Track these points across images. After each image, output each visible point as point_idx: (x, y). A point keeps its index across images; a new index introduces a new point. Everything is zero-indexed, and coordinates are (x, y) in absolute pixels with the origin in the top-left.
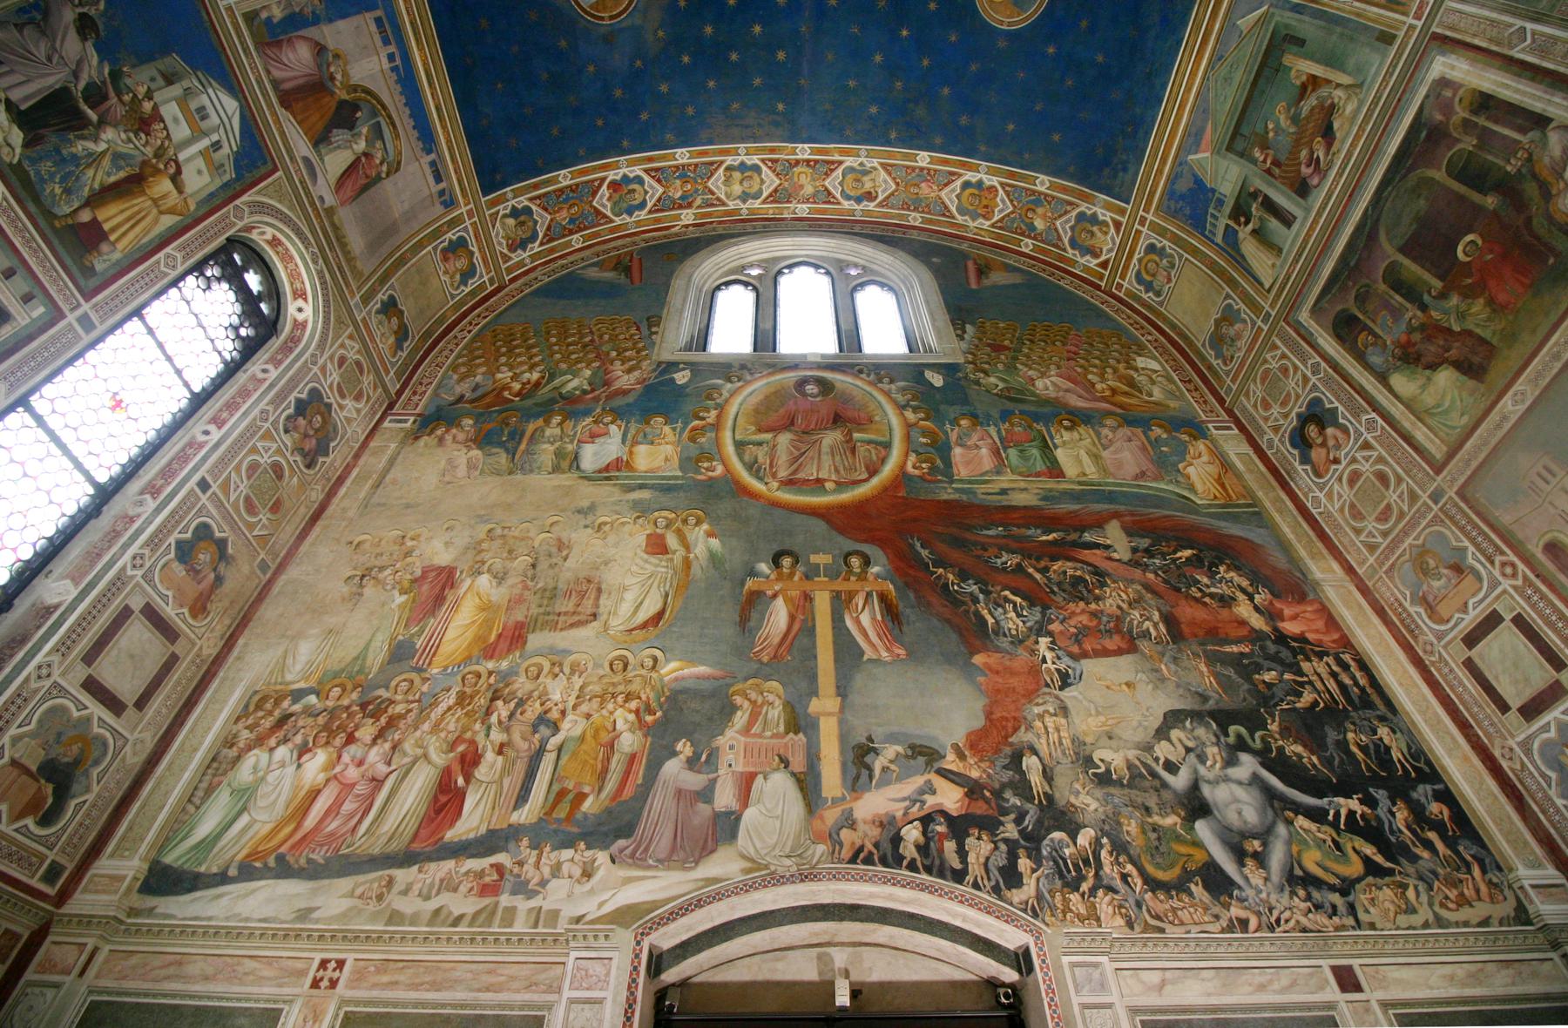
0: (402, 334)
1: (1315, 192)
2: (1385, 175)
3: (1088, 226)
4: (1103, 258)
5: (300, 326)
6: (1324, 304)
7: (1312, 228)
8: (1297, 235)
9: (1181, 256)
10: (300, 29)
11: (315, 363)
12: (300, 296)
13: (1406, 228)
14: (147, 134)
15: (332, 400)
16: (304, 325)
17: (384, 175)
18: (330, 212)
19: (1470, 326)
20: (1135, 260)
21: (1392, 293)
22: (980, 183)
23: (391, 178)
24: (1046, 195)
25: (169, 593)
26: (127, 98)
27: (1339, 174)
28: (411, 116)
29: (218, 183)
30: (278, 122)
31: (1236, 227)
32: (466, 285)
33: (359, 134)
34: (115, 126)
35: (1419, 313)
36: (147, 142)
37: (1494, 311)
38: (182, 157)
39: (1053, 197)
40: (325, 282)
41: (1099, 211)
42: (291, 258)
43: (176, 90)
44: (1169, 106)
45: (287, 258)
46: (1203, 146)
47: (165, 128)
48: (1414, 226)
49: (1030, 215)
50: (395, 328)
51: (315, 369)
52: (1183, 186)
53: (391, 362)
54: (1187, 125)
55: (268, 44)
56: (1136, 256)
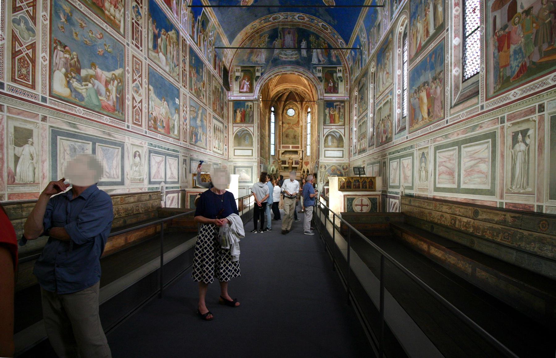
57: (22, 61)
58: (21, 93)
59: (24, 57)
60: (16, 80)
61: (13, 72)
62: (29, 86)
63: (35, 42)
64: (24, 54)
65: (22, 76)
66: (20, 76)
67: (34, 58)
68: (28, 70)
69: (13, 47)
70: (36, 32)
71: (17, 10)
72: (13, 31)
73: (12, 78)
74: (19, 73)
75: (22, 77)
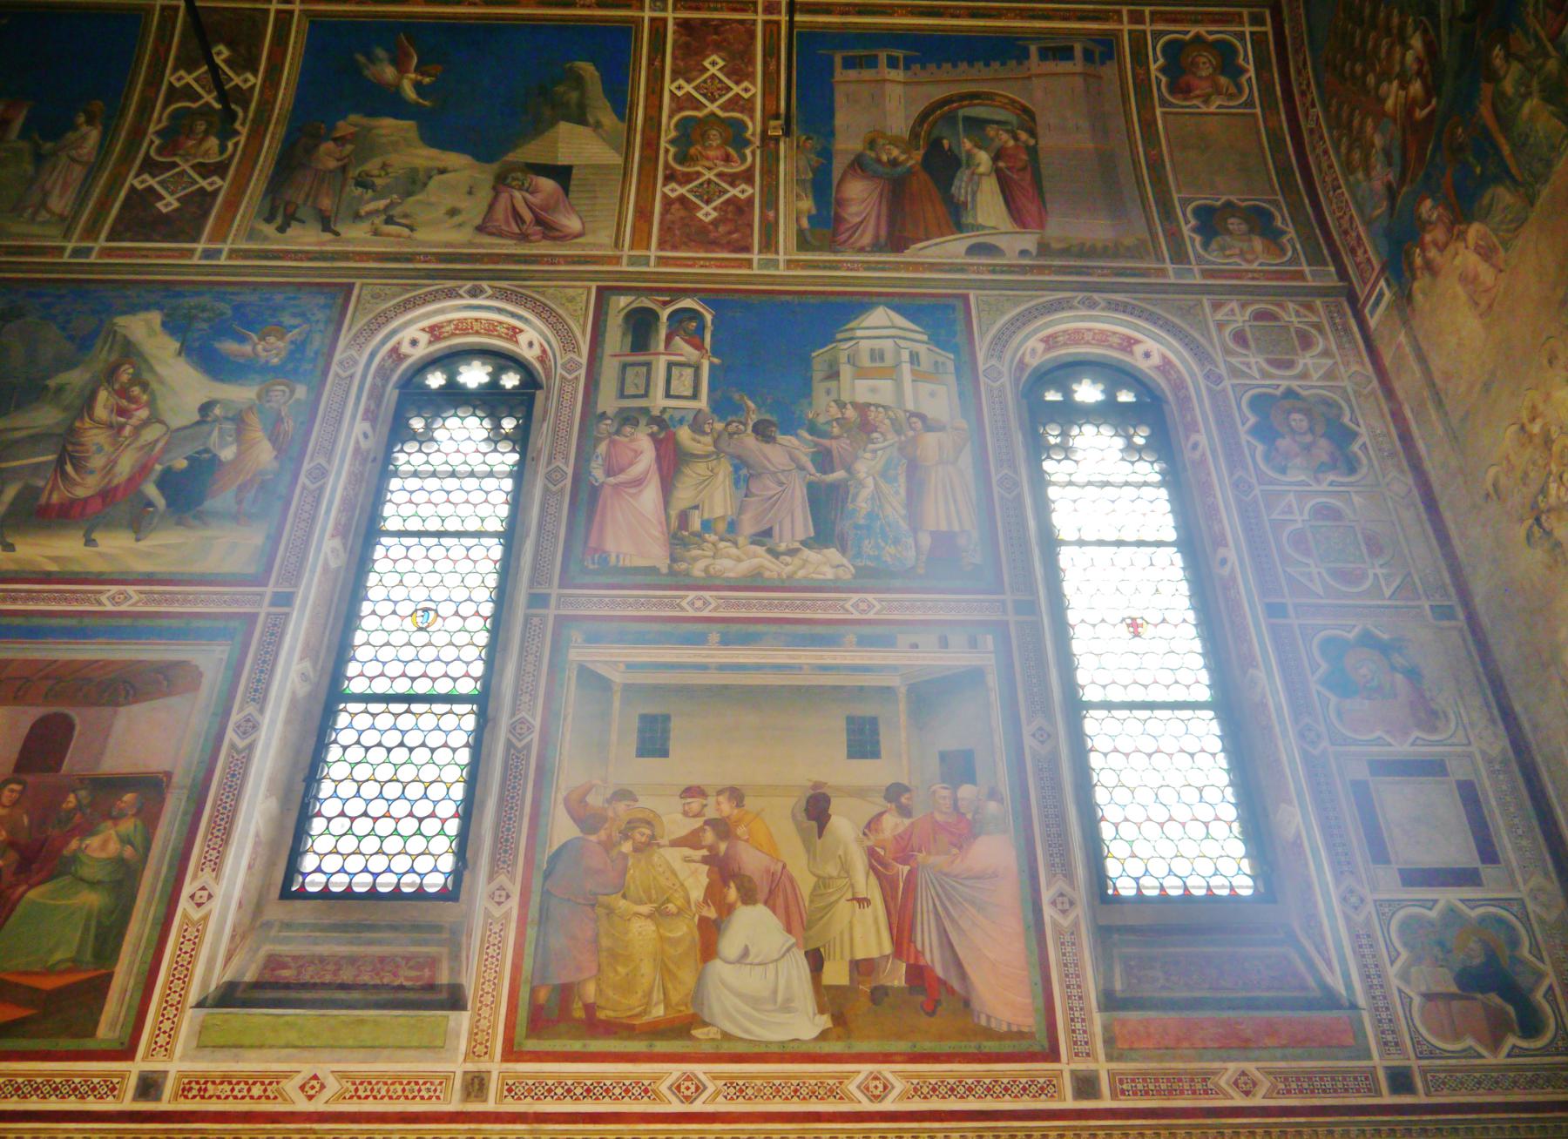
0: (1260, 221)
5: (1166, 366)
10: (830, 183)
11: (1220, 379)
12: (1131, 345)
14: (875, 429)
15: (1285, 384)
16: (1166, 361)
17: (1032, 142)
18: (1044, 249)
23: (1040, 131)
25: (1378, 734)
26: (836, 431)
28: (971, 63)
29: (951, 379)
30: (917, 266)
32: (1243, 71)
33: (970, 155)
34: (856, 458)
36: (882, 434)
38: (910, 406)
40: (1126, 305)
42: (1077, 331)
43: (846, 371)
45: (1076, 337)
47: (877, 406)
50: (1244, 227)
51: (1227, 383)
53: (1290, 262)
55: (835, 234)
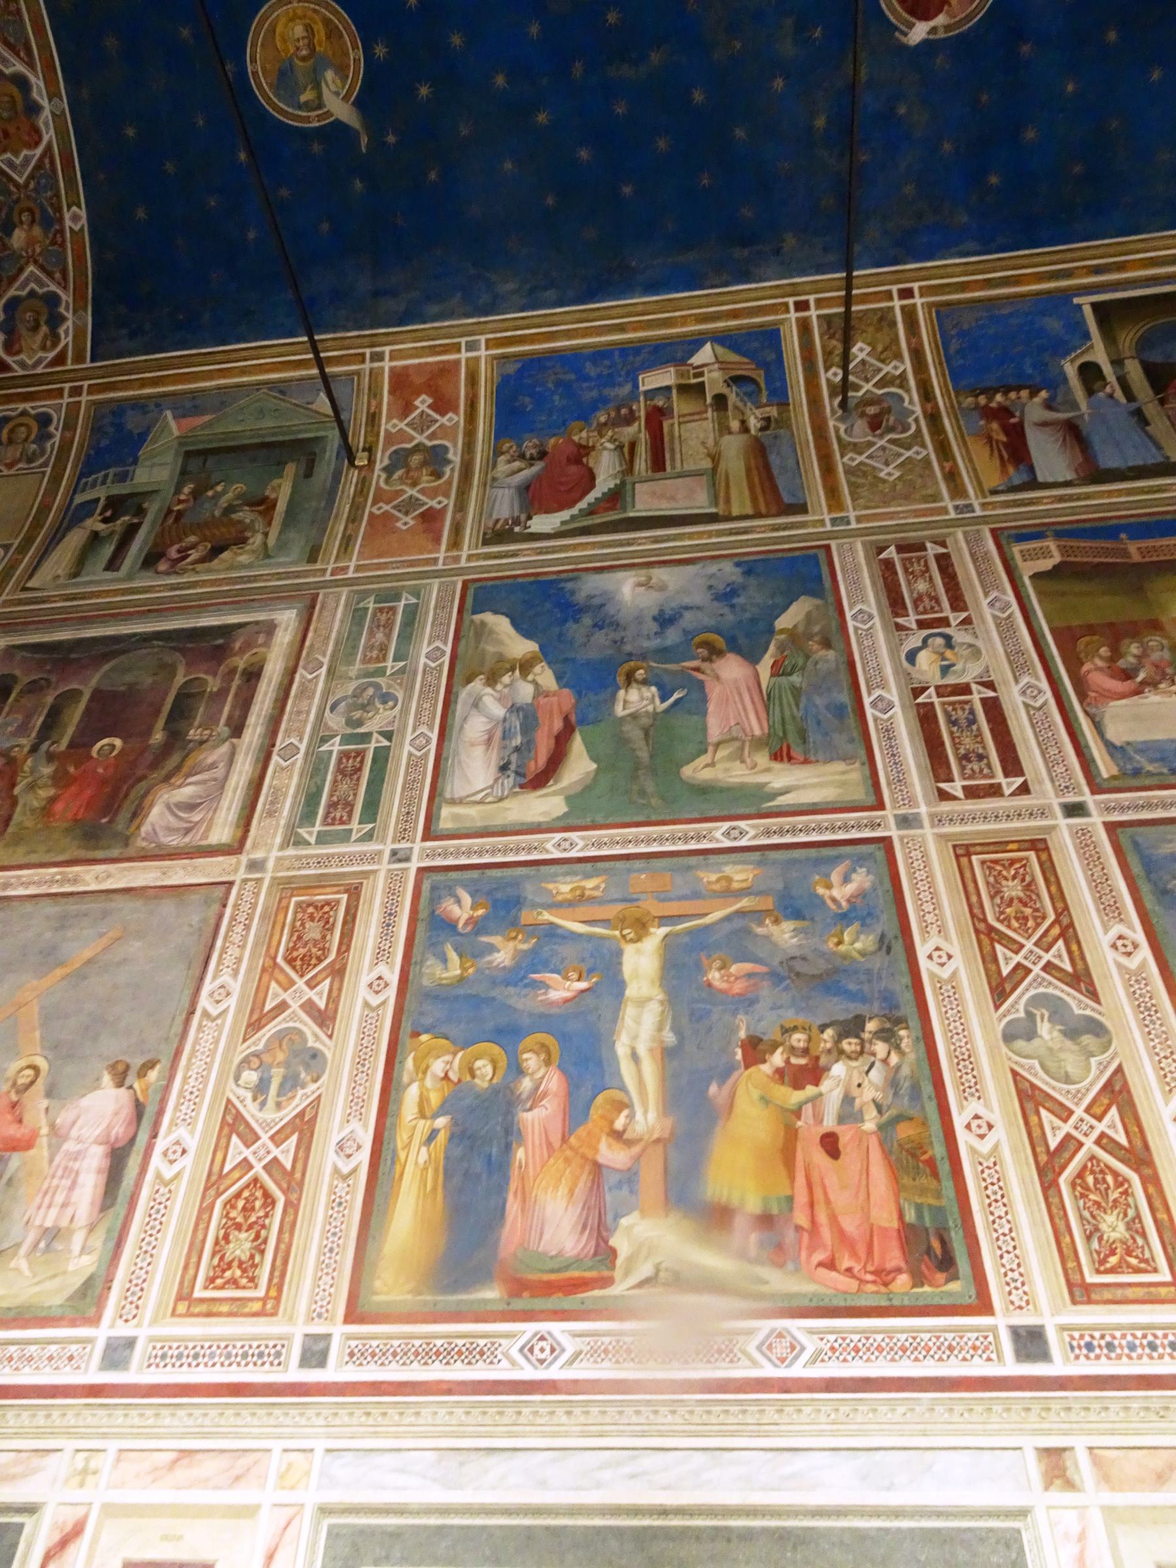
1: (150, 574)
2: (169, 632)
3: (43, 319)
4: (9, 360)
6: (19, 655)
7: (107, 593)
8: (99, 582)
9: (45, 464)
13: (120, 683)
19: (21, 802)
20: (22, 406)
21: (45, 711)
22: (34, 109)
24: (62, 232)
27: (173, 587)
31: (98, 511)
35: (26, 750)
37: (43, 808)
39: (63, 245)
41: (70, 323)
44: (219, 357)
46: (184, 421)
48: (123, 688)
49: (25, 217)
52: (132, 422)
54: (203, 390)
56: (27, 406)
57: (1090, 1180)
58: (1132, 1347)
59: (1092, 1158)
60: (1088, 1288)
61: (1066, 1254)
62: (1163, 1291)
63: (1119, 1070)
64: (1089, 1144)
65: (1113, 1252)
66: (1103, 1262)
67: (1138, 1143)
68: (1131, 1213)
69: (1036, 1138)
70: (1108, 1024)
71: (1008, 987)
72: (1015, 1074)
73: (1070, 1285)
74: (1095, 1245)
75: (1113, 1260)
